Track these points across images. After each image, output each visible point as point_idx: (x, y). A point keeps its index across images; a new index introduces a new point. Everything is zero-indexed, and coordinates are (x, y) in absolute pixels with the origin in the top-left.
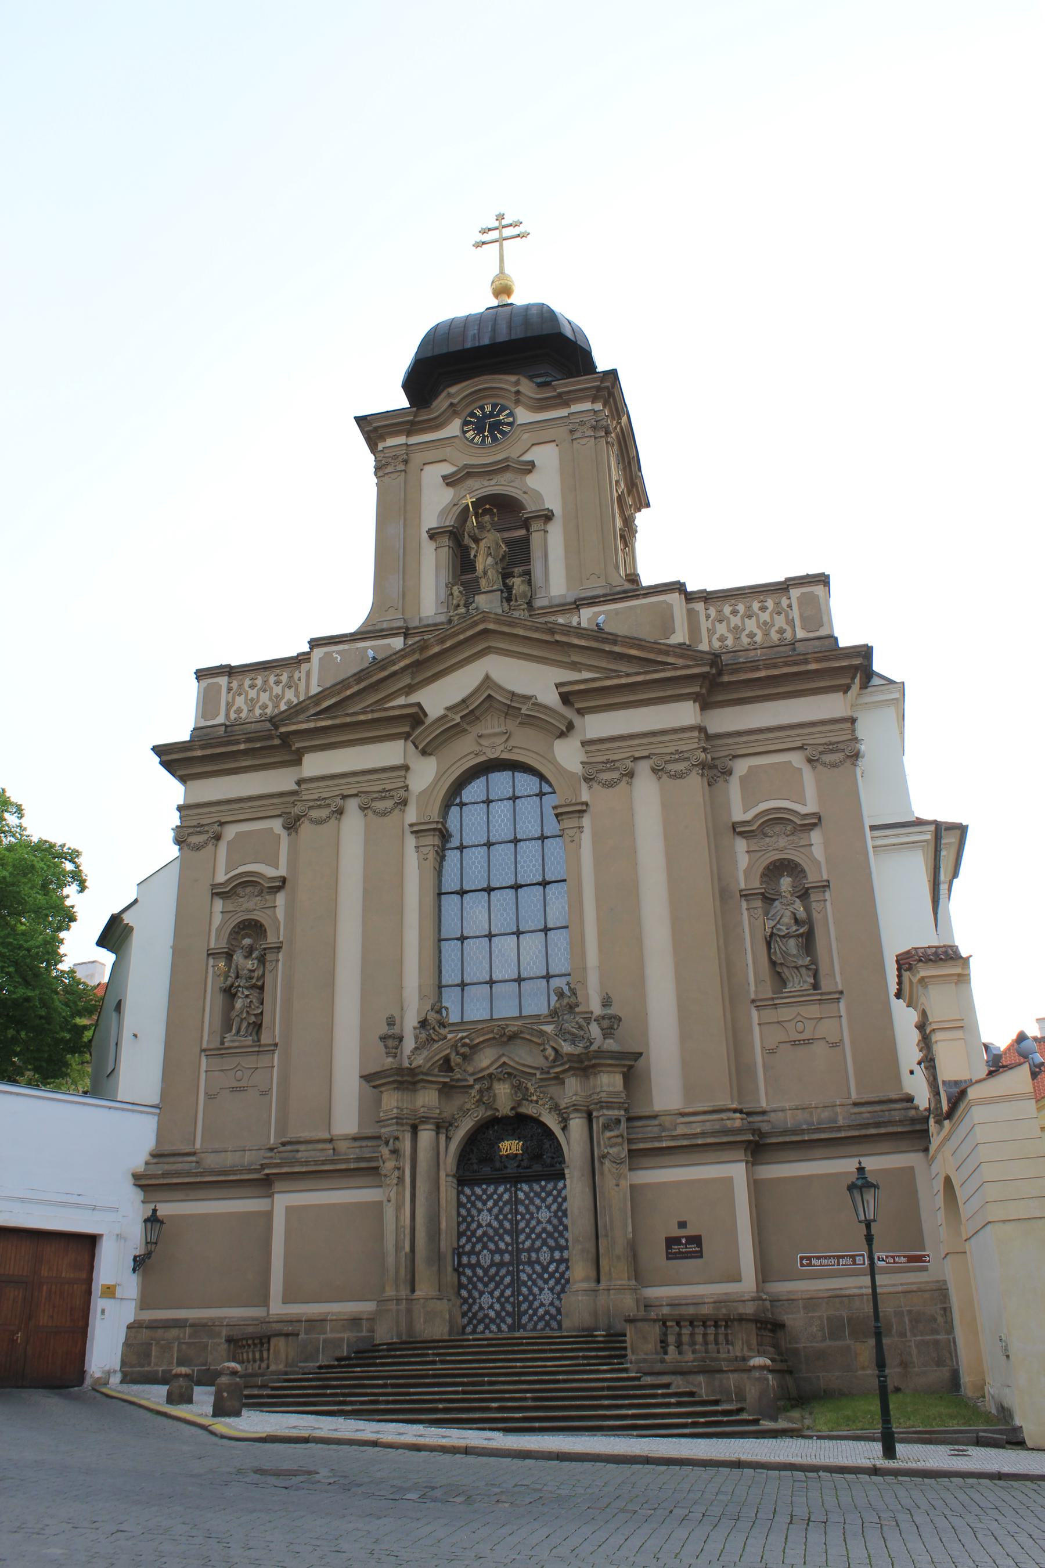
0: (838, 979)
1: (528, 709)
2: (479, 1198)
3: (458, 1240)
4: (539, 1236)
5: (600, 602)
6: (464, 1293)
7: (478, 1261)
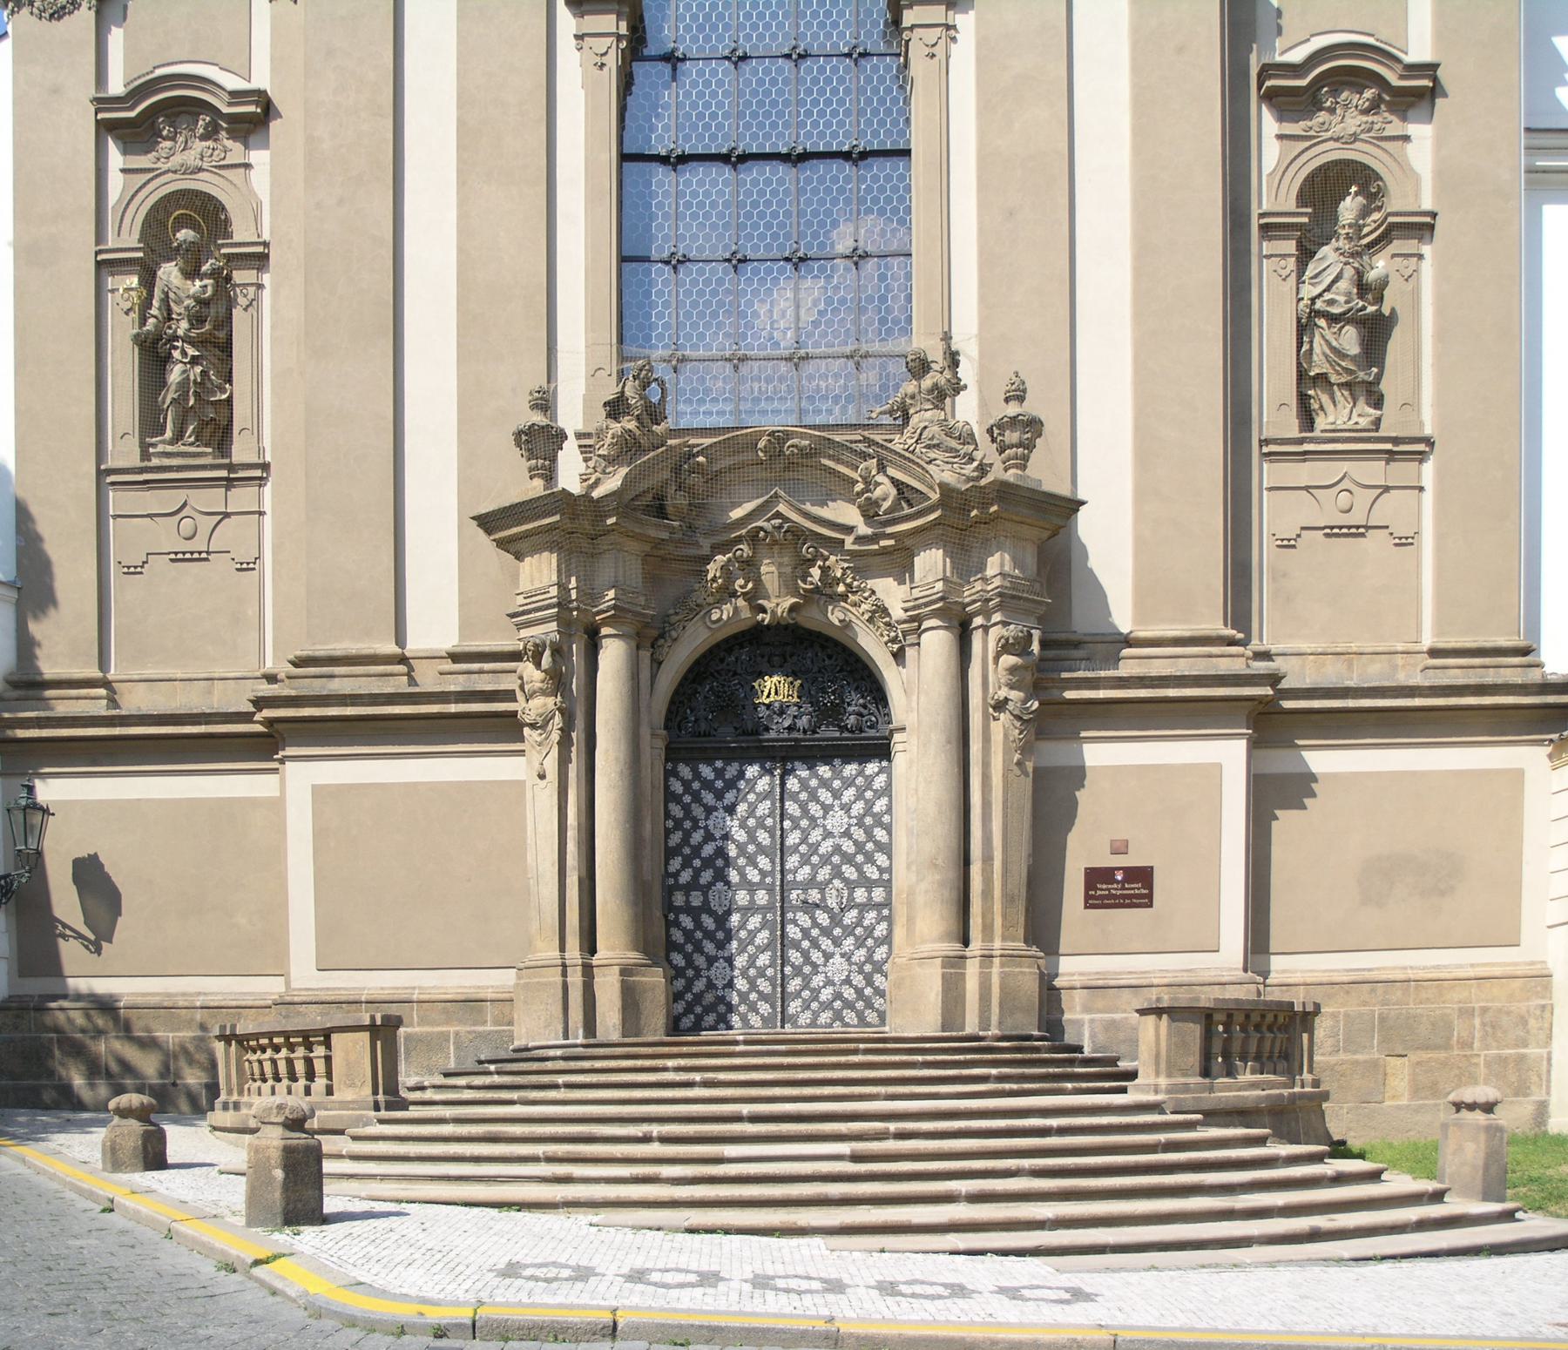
2: (708, 785)
3: (667, 864)
7: (706, 902)
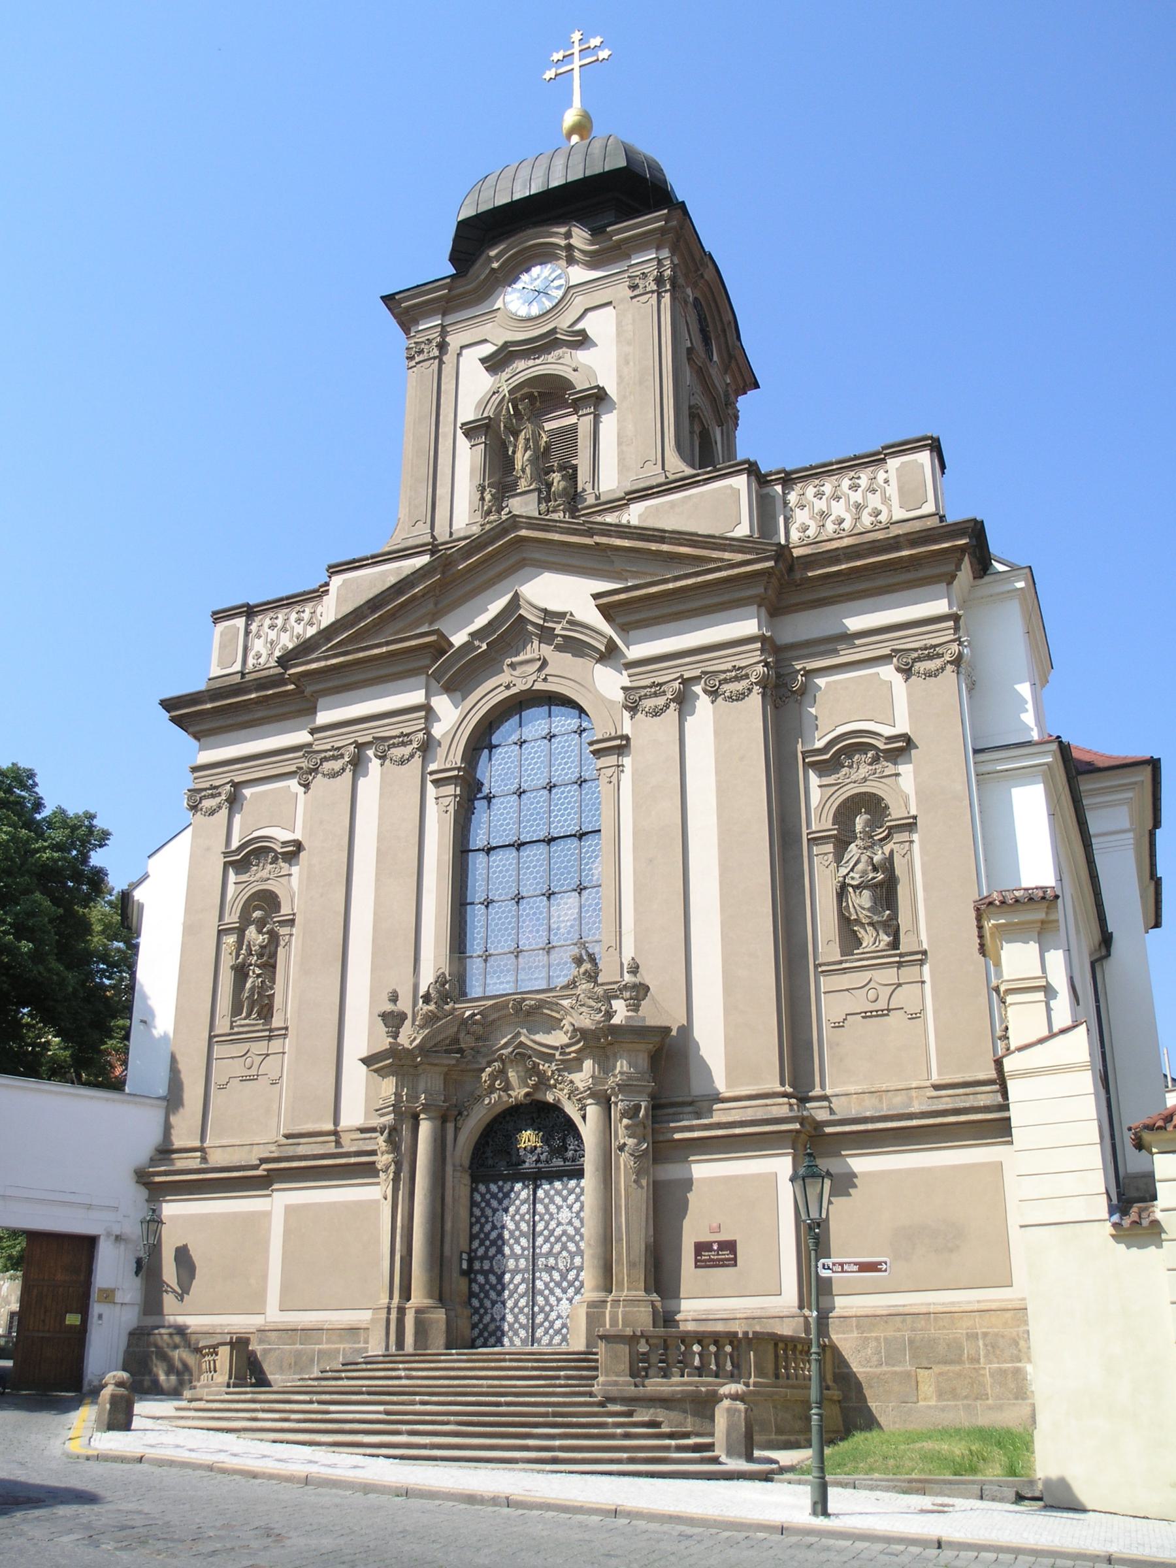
0: (923, 936)
1: (563, 629)
2: (494, 1196)
3: (471, 1243)
4: (558, 1239)
5: (653, 493)
6: (476, 1303)
